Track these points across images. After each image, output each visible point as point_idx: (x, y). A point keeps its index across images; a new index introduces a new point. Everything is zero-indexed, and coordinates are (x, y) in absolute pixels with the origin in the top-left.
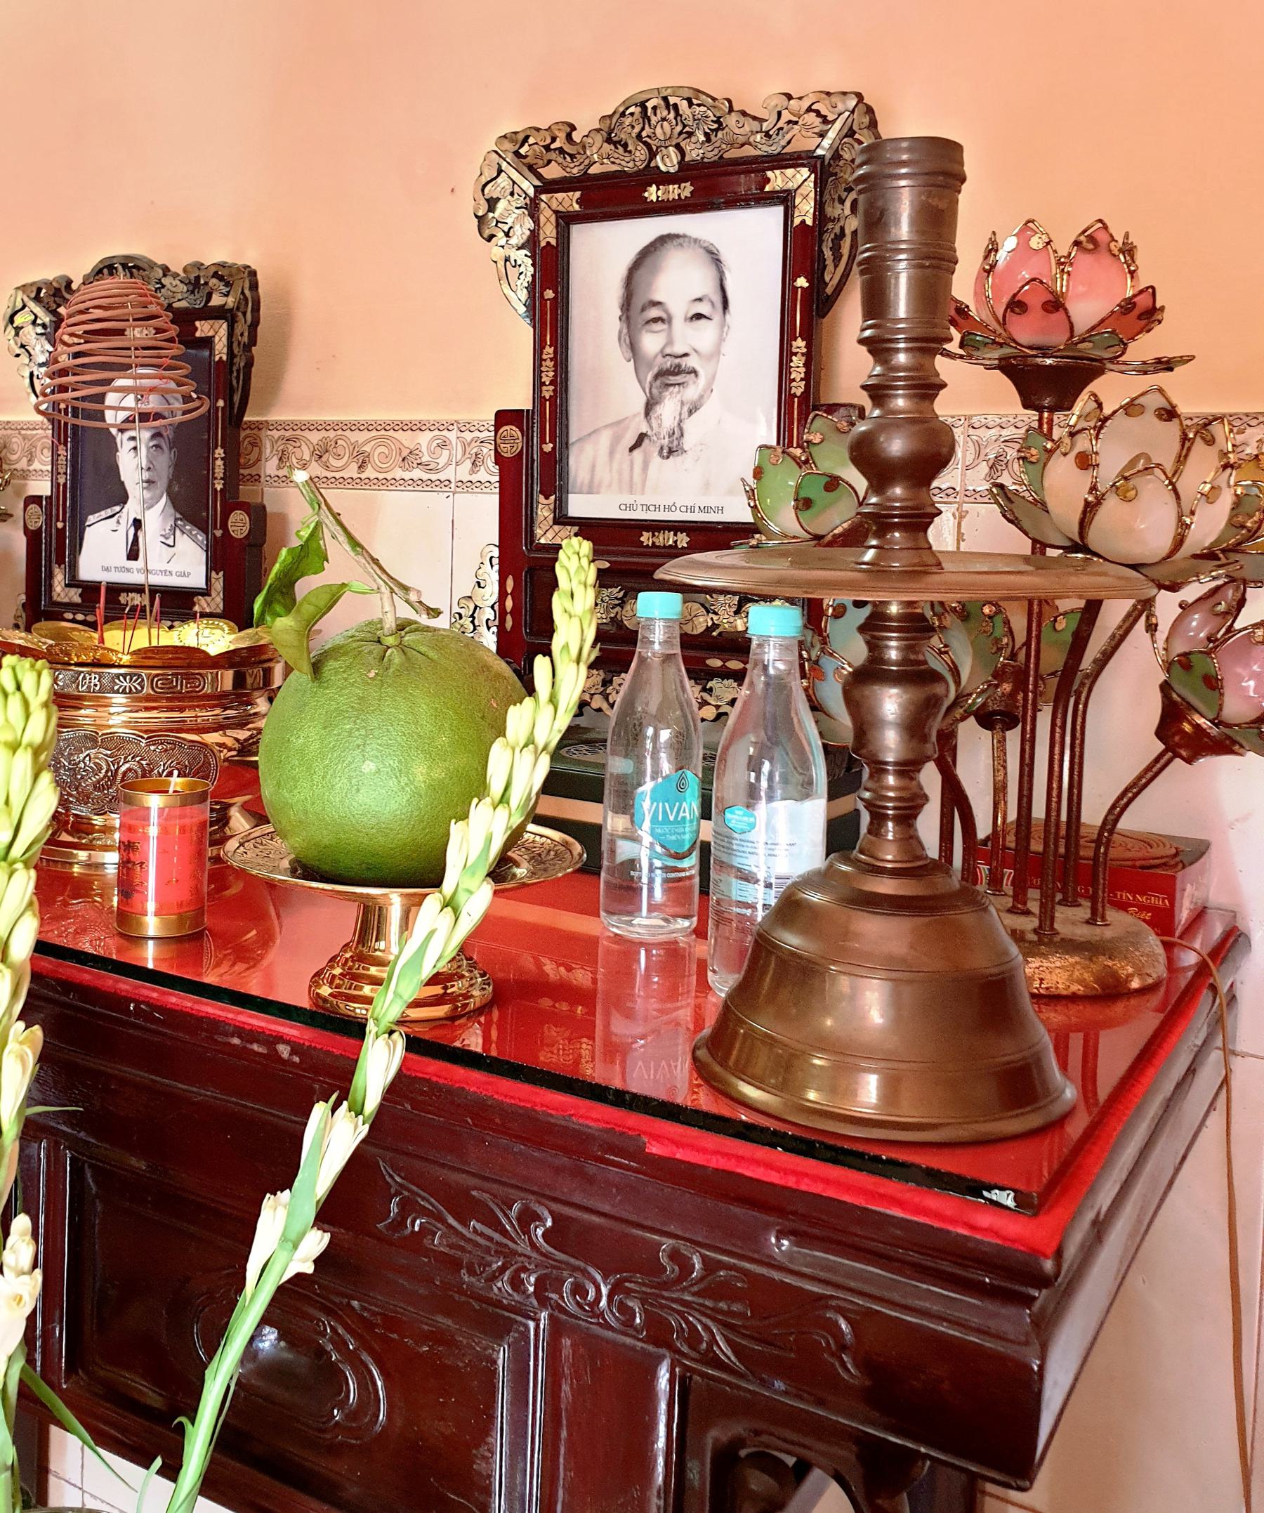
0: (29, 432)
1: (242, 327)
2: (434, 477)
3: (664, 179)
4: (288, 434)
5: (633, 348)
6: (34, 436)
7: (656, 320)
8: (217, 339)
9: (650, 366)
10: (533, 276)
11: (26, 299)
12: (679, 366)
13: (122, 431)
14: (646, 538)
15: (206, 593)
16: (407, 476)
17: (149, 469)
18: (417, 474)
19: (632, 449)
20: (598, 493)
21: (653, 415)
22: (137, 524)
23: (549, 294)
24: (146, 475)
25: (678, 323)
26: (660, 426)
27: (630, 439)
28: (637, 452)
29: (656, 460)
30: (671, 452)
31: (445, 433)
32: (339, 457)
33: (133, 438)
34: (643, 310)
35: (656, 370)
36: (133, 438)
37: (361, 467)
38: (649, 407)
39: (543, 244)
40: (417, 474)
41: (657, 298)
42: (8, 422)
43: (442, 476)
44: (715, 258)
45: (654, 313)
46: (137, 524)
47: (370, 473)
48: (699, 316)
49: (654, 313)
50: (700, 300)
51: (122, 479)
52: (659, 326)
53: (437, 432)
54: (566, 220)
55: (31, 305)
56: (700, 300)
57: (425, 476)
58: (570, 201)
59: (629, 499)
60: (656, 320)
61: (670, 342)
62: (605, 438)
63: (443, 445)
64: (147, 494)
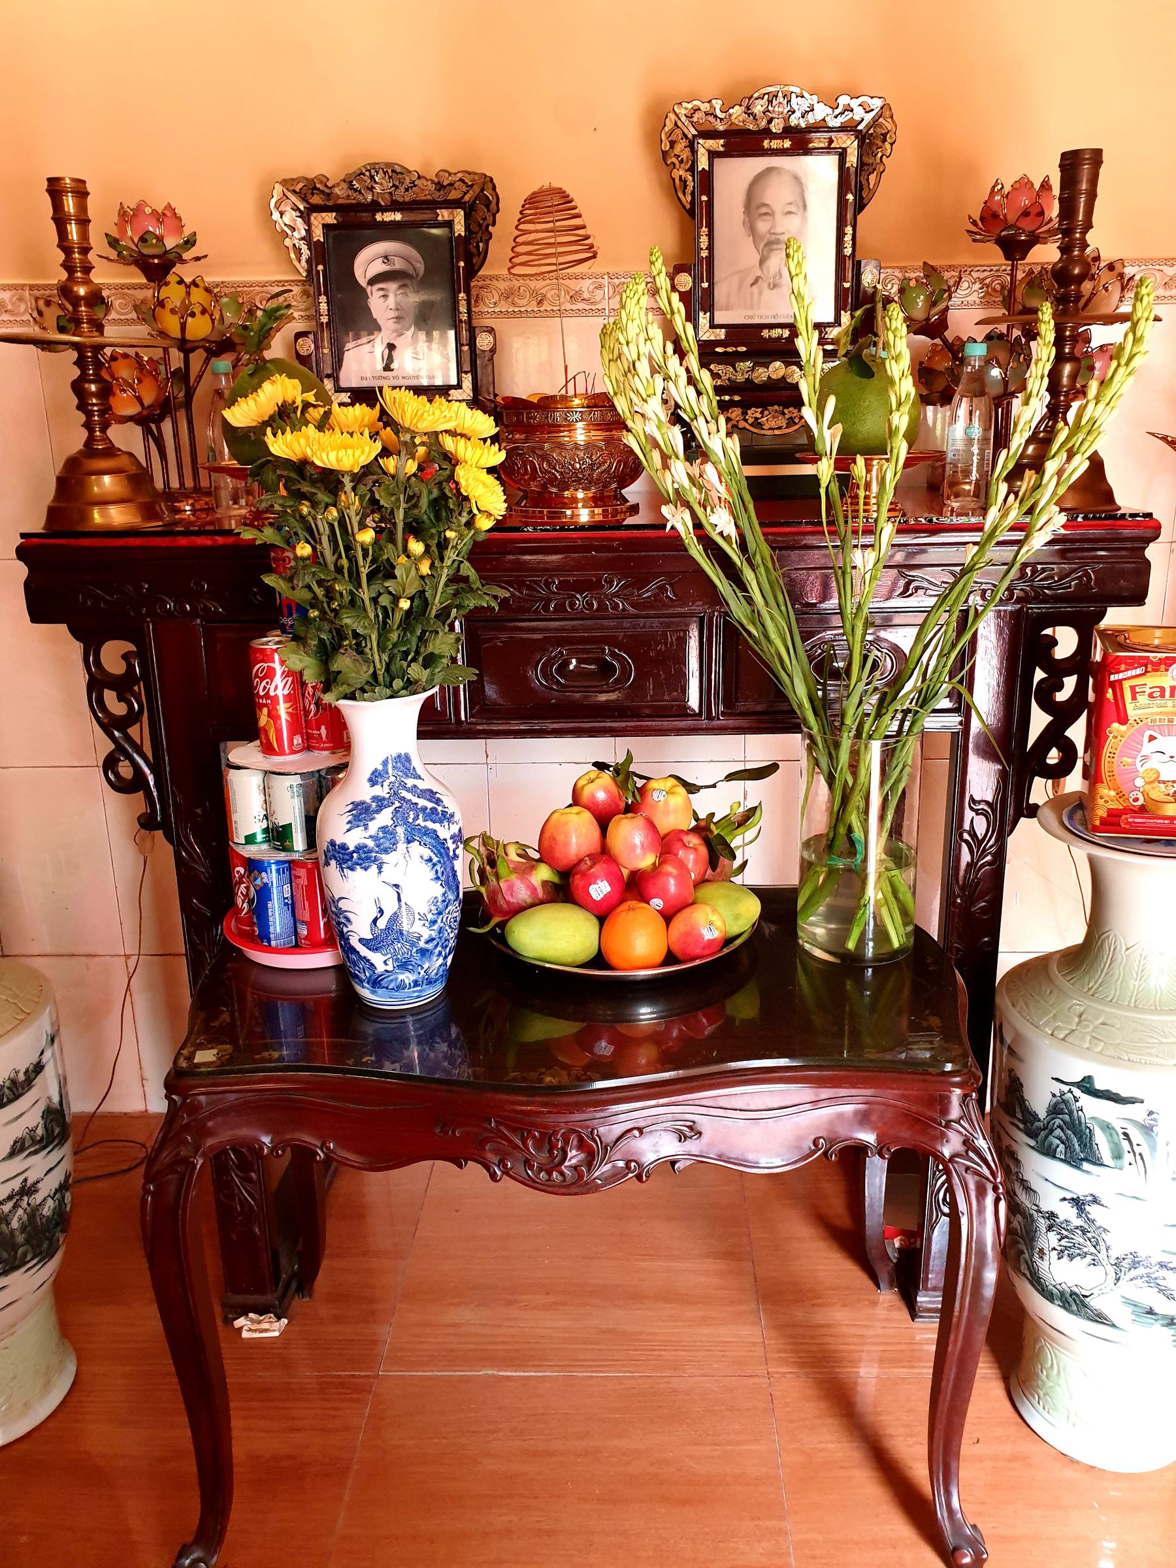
0: (245, 289)
1: (478, 216)
2: (594, 307)
3: (775, 136)
4: (480, 284)
5: (752, 230)
6: (252, 291)
7: (766, 214)
8: (456, 221)
9: (762, 238)
10: (694, 187)
11: (285, 190)
12: (779, 239)
13: (372, 282)
14: (765, 333)
15: (459, 386)
16: (574, 307)
17: (397, 309)
18: (581, 306)
19: (752, 285)
20: (732, 309)
21: (765, 266)
22: (391, 347)
23: (704, 198)
24: (396, 314)
25: (778, 215)
26: (768, 272)
27: (751, 280)
28: (754, 287)
29: (766, 291)
30: (775, 286)
31: (600, 280)
32: (522, 297)
33: (382, 289)
34: (758, 208)
35: (765, 242)
36: (382, 289)
37: (540, 303)
38: (762, 262)
39: (700, 169)
40: (581, 306)
41: (767, 202)
42: (223, 282)
43: (599, 306)
44: (797, 179)
45: (764, 210)
46: (391, 347)
47: (546, 306)
48: (790, 213)
49: (764, 210)
50: (790, 204)
51: (374, 317)
52: (768, 217)
53: (594, 280)
54: (713, 155)
55: (289, 194)
56: (790, 204)
57: (587, 307)
58: (717, 144)
59: (750, 313)
60: (766, 214)
61: (773, 226)
62: (735, 280)
63: (600, 287)
64: (398, 326)
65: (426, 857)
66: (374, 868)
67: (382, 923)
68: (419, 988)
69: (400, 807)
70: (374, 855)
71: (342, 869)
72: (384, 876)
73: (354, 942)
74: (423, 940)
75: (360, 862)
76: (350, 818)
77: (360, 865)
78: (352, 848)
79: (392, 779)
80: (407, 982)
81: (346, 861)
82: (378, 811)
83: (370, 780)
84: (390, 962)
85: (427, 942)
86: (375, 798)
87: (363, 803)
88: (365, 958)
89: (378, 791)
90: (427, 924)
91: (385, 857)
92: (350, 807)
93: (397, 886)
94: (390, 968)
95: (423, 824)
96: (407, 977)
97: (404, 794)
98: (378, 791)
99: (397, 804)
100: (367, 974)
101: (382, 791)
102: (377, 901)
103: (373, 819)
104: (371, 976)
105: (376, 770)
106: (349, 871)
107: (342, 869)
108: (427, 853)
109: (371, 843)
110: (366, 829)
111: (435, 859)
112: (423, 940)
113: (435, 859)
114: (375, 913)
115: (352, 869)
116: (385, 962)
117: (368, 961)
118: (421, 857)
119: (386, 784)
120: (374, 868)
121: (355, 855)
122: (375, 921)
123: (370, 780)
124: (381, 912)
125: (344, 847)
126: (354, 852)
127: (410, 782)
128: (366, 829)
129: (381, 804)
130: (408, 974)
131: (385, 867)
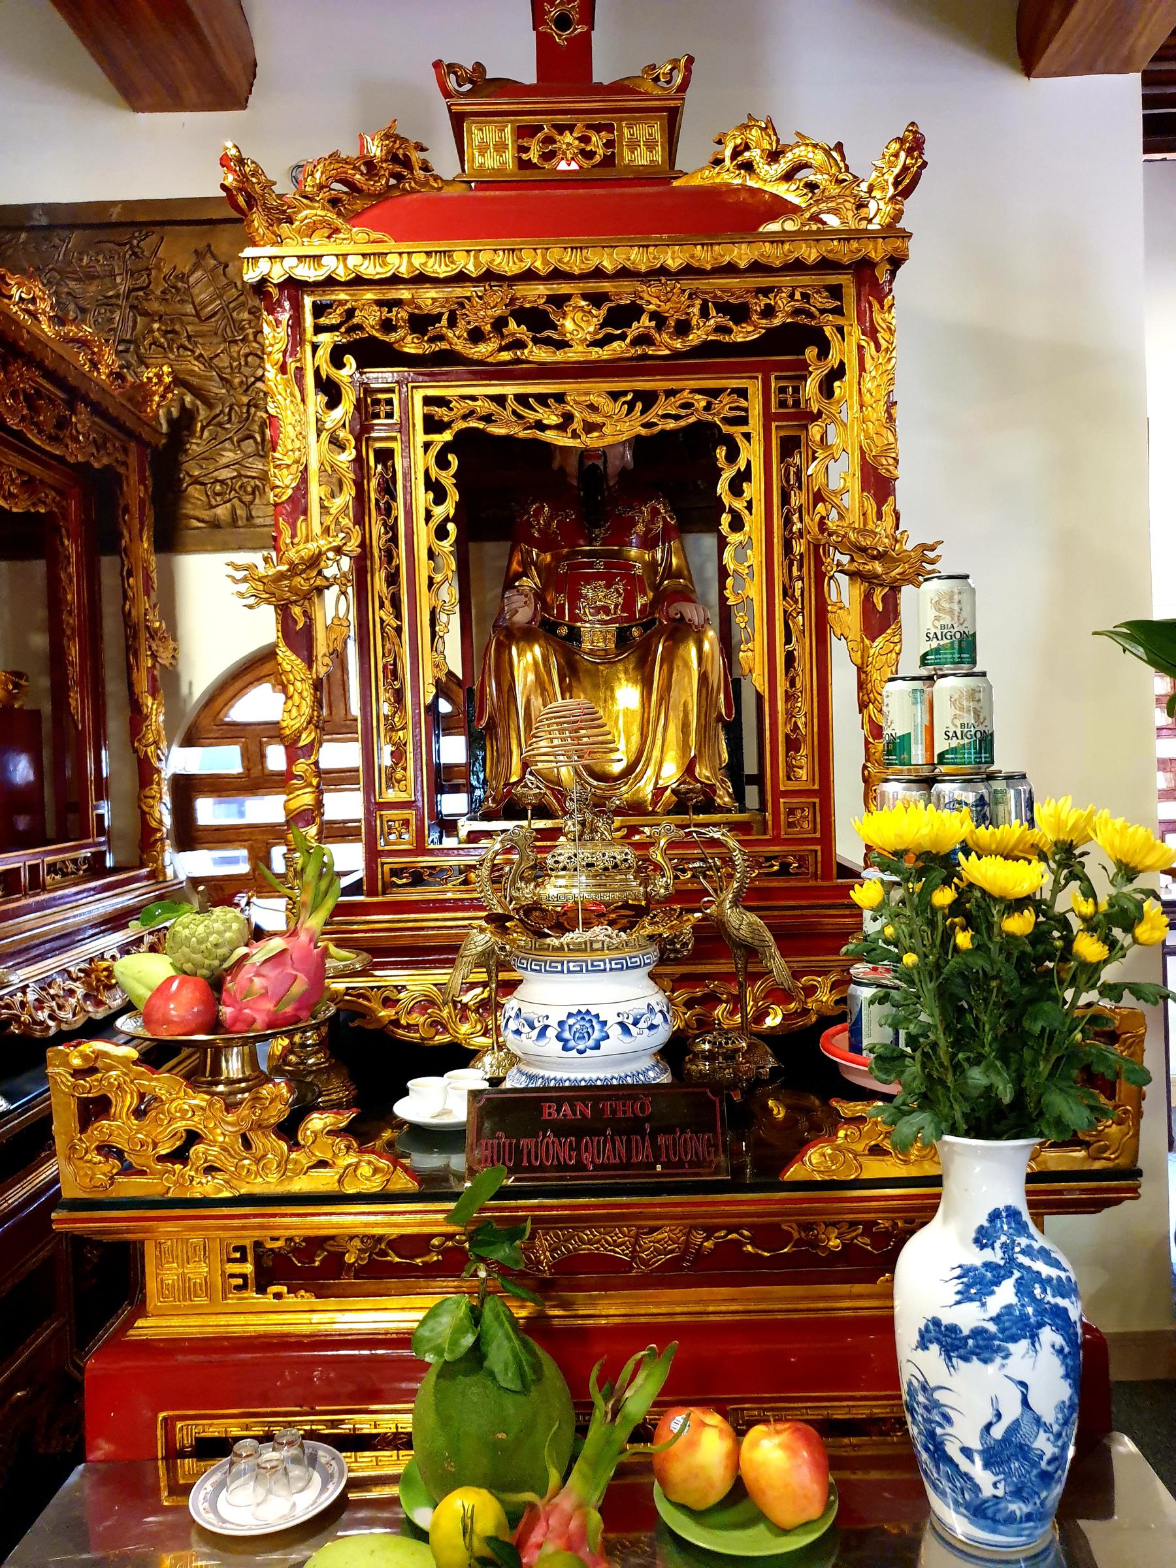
65: (1057, 1347)
67: (998, 1432)
68: (1031, 1524)
69: (1022, 1278)
70: (997, 1343)
71: (950, 1358)
72: (1006, 1371)
73: (952, 1450)
74: (1045, 1458)
75: (978, 1351)
76: (960, 1287)
77: (977, 1355)
78: (966, 1332)
79: (1003, 1238)
80: (1018, 1513)
81: (957, 1348)
82: (997, 1283)
83: (977, 1241)
84: (1001, 1486)
85: (1049, 1462)
86: (987, 1265)
88: (966, 1474)
89: (989, 1255)
90: (1052, 1438)
91: (1011, 1347)
92: (958, 1272)
93: (1023, 1384)
94: (1000, 1493)
95: (1053, 1301)
96: (1020, 1509)
97: (1021, 1259)
98: (989, 1255)
99: (1017, 1274)
100: (967, 1496)
101: (995, 1256)
102: (994, 1401)
103: (992, 1293)
104: (972, 1499)
105: (982, 1227)
106: (961, 1363)
107: (950, 1358)
108: (1059, 1340)
109: (992, 1328)
111: (1067, 1350)
112: (1045, 1458)
113: (1067, 1350)
114: (989, 1416)
115: (966, 1359)
116: (995, 1485)
117: (970, 1479)
118: (1053, 1346)
119: (997, 1245)
120: (998, 1360)
121: (971, 1342)
122: (988, 1427)
123: (977, 1241)
124: (999, 1416)
125: (953, 1329)
126: (969, 1337)
127: (1024, 1241)
128: (983, 1305)
129: (998, 1273)
130: (1022, 1505)
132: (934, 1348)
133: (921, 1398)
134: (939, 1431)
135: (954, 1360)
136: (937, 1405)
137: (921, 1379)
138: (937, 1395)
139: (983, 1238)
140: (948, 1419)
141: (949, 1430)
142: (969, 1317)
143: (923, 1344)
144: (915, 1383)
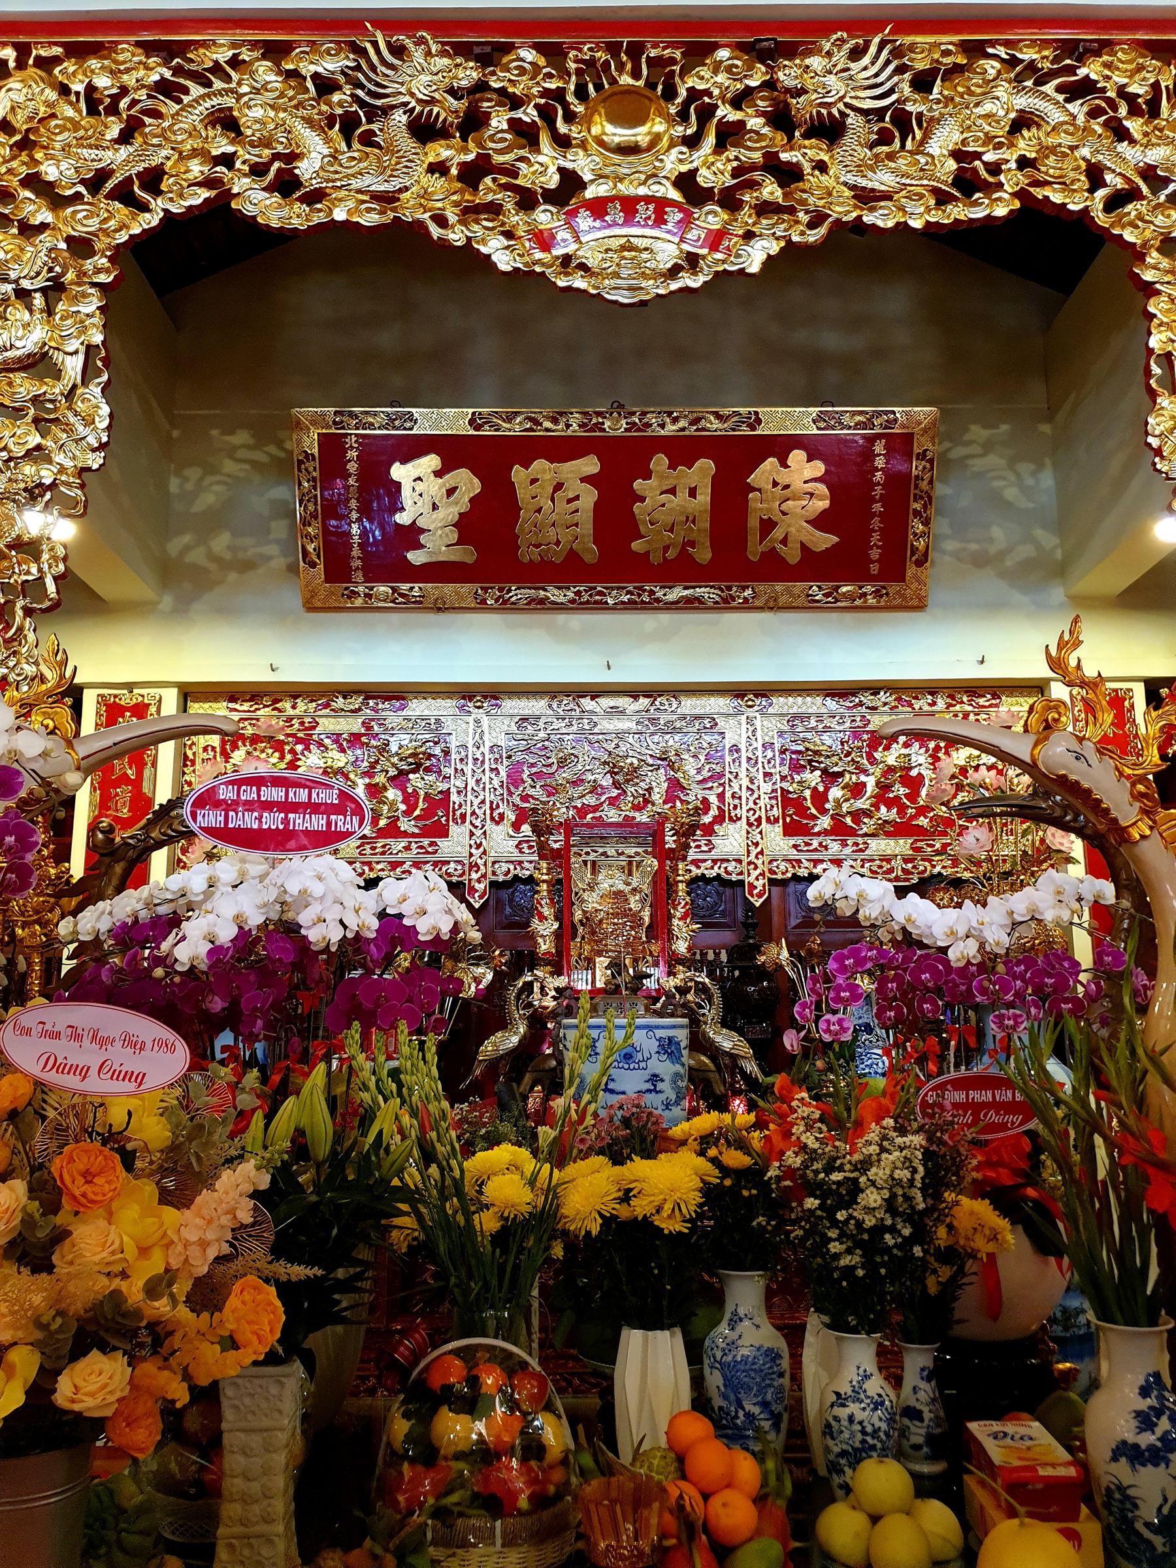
66: (1163, 1465)
72: (1170, 1471)
73: (1139, 1526)
78: (1143, 1447)
86: (1151, 1408)
87: (1142, 1412)
91: (1171, 1456)
101: (1151, 1401)
109: (1159, 1444)
110: (1153, 1433)
114: (1160, 1500)
115: (1144, 1465)
119: (1153, 1396)
120: (1163, 1465)
124: (1165, 1500)
125: (1136, 1446)
129: (1159, 1412)
131: (1171, 1464)
132: (1123, 1460)
133: (1117, 1496)
134: (1130, 1515)
135: (1137, 1466)
136: (1129, 1498)
137: (1116, 1482)
138: (1131, 1492)
139: (1144, 1392)
140: (1136, 1506)
141: (1137, 1513)
142: (1147, 1439)
143: (1115, 1459)
144: (1112, 1487)
